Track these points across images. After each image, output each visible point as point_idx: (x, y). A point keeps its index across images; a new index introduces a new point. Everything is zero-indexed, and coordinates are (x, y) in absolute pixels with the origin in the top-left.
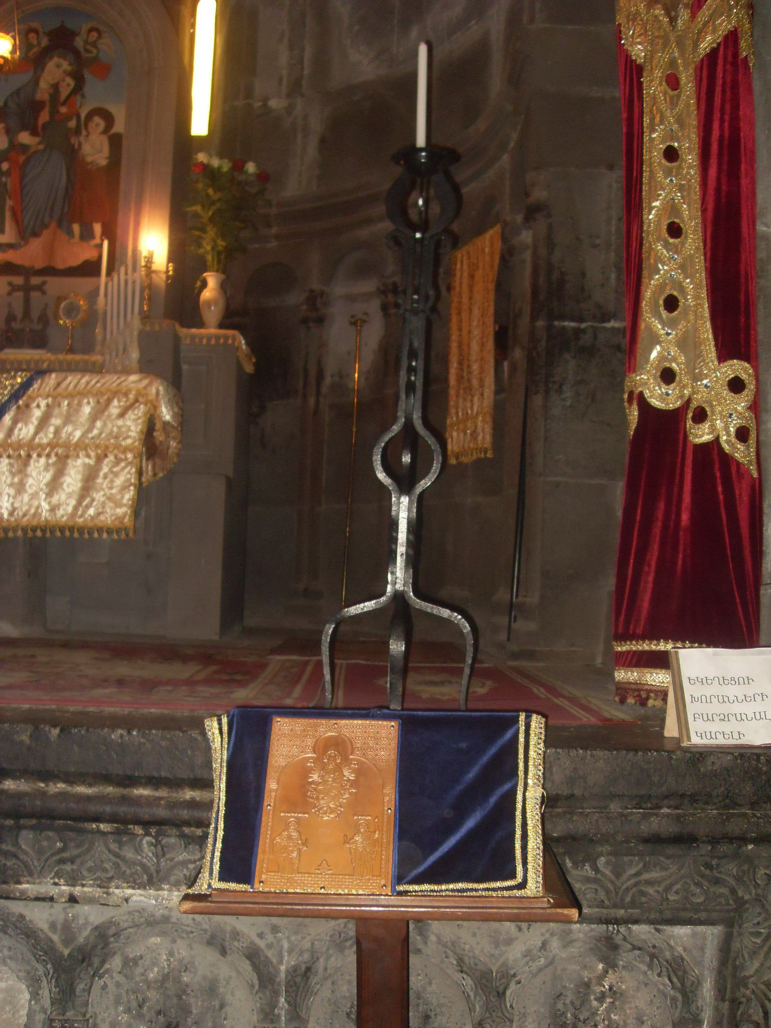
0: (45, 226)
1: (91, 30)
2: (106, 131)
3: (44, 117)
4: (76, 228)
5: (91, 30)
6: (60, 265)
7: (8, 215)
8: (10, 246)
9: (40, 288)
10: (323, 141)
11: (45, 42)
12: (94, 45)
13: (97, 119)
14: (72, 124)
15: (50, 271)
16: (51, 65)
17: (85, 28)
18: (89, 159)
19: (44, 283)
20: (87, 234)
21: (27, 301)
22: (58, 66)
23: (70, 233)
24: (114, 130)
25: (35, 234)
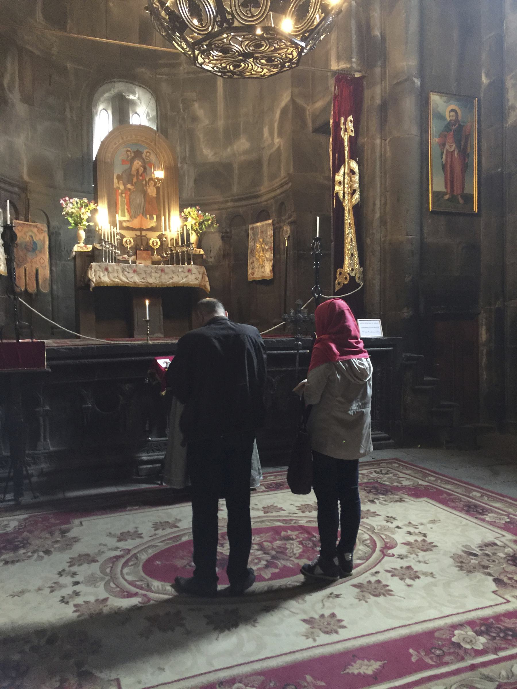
0: (138, 215)
1: (147, 152)
3: (135, 180)
4: (148, 216)
5: (147, 152)
6: (144, 228)
7: (126, 211)
8: (128, 221)
9: (145, 236)
10: (195, 180)
11: (133, 155)
12: (149, 157)
14: (144, 182)
17: (145, 151)
20: (152, 218)
23: (146, 218)
25: (135, 217)
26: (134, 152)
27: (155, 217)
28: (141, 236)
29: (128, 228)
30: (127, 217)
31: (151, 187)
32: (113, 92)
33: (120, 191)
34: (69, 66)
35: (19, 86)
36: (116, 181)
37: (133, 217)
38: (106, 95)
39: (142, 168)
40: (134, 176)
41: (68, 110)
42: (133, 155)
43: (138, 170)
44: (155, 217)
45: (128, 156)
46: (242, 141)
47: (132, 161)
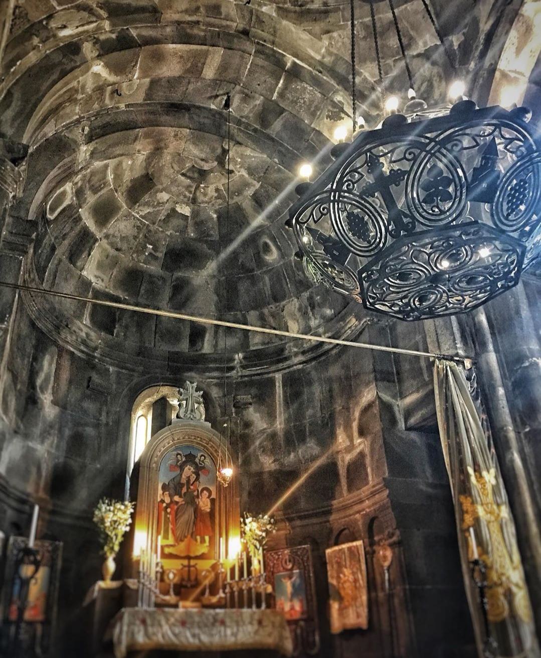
0: (185, 537)
2: (209, 497)
3: (184, 490)
4: (198, 538)
5: (202, 456)
6: (192, 555)
9: (194, 566)
11: (184, 459)
12: (203, 462)
13: (205, 492)
14: (196, 493)
15: (189, 558)
16: (186, 469)
17: (199, 455)
18: (203, 509)
19: (196, 564)
20: (203, 541)
21: (189, 571)
22: (189, 469)
23: (196, 540)
24: (212, 497)
25: (182, 540)
26: (186, 456)
27: (207, 538)
28: (189, 566)
29: (171, 556)
30: (171, 541)
31: (204, 499)
32: (156, 397)
33: (164, 505)
34: (111, 369)
35: (53, 387)
36: (160, 492)
37: (179, 540)
38: (148, 400)
39: (194, 476)
40: (183, 485)
41: (104, 414)
42: (184, 459)
43: (189, 478)
44: (207, 538)
45: (178, 461)
46: (308, 445)
47: (182, 468)
